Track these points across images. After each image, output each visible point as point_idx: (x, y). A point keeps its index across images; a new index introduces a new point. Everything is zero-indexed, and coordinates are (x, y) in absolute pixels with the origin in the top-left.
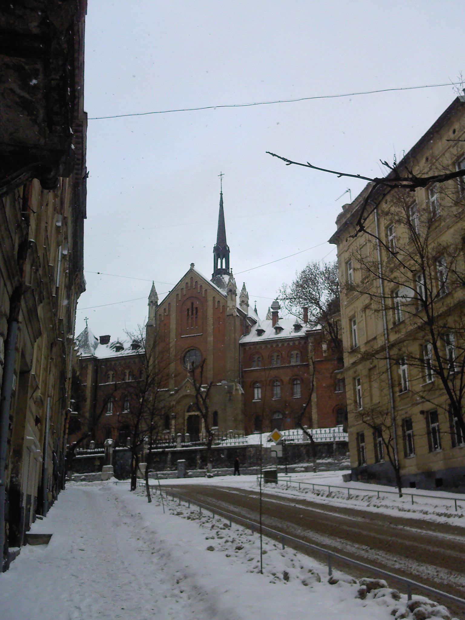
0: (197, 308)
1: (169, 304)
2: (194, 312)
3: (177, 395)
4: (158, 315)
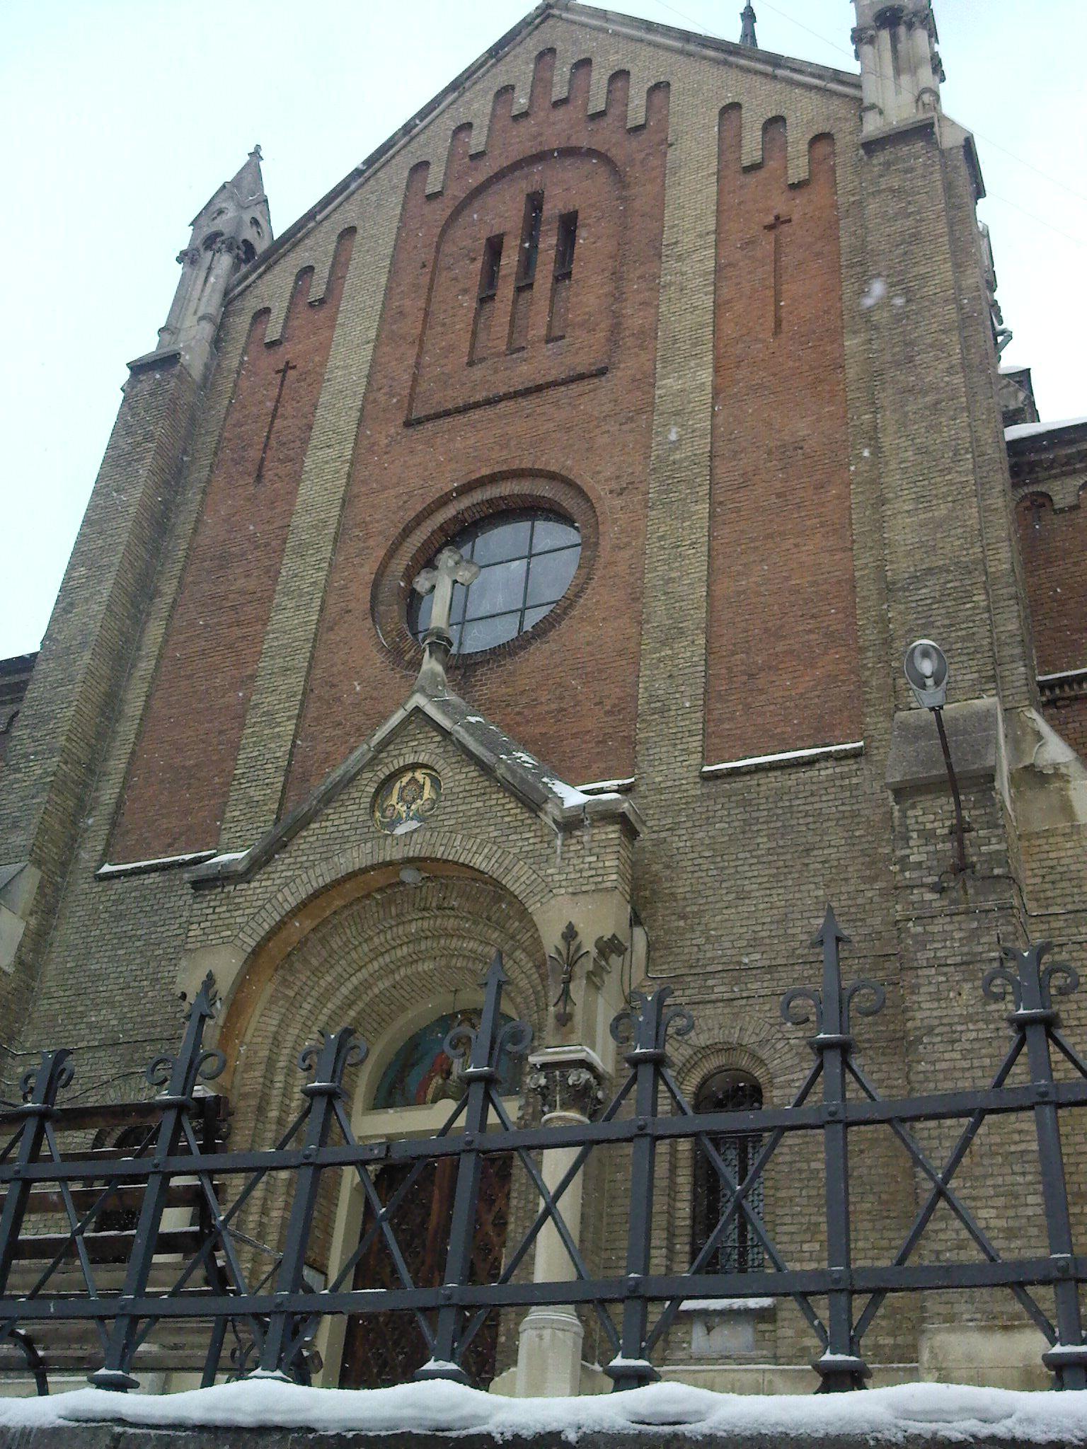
0: (569, 224)
1: (351, 231)
2: (549, 242)
3: (282, 865)
4: (242, 323)
